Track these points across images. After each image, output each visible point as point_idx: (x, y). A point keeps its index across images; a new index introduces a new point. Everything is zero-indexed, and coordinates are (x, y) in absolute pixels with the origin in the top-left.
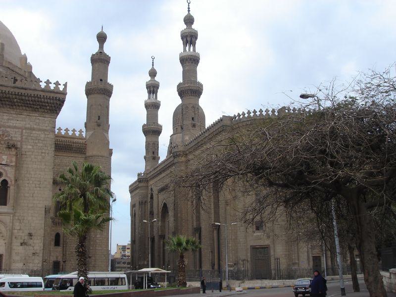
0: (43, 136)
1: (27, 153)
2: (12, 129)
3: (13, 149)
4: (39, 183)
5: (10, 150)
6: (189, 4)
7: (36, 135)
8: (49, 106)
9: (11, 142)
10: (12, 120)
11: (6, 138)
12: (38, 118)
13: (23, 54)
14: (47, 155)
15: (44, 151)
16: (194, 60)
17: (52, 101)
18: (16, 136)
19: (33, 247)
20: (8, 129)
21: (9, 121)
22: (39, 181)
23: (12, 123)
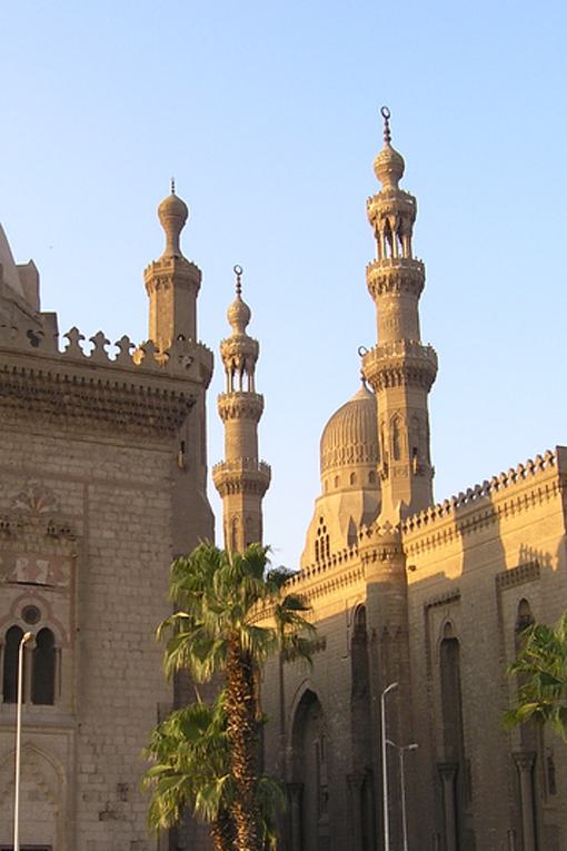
0: (140, 502)
1: (102, 553)
2: (60, 484)
3: (64, 541)
4: (138, 637)
5: (56, 541)
6: (387, 118)
7: (121, 500)
8: (153, 416)
9: (60, 522)
10: (57, 455)
11: (46, 509)
12: (125, 450)
13: (20, 259)
14: (155, 558)
15: (145, 547)
16: (413, 283)
17: (162, 404)
18: (71, 503)
19: (132, 822)
20: (49, 483)
21: (51, 459)
22: (136, 633)
23: (58, 465)
